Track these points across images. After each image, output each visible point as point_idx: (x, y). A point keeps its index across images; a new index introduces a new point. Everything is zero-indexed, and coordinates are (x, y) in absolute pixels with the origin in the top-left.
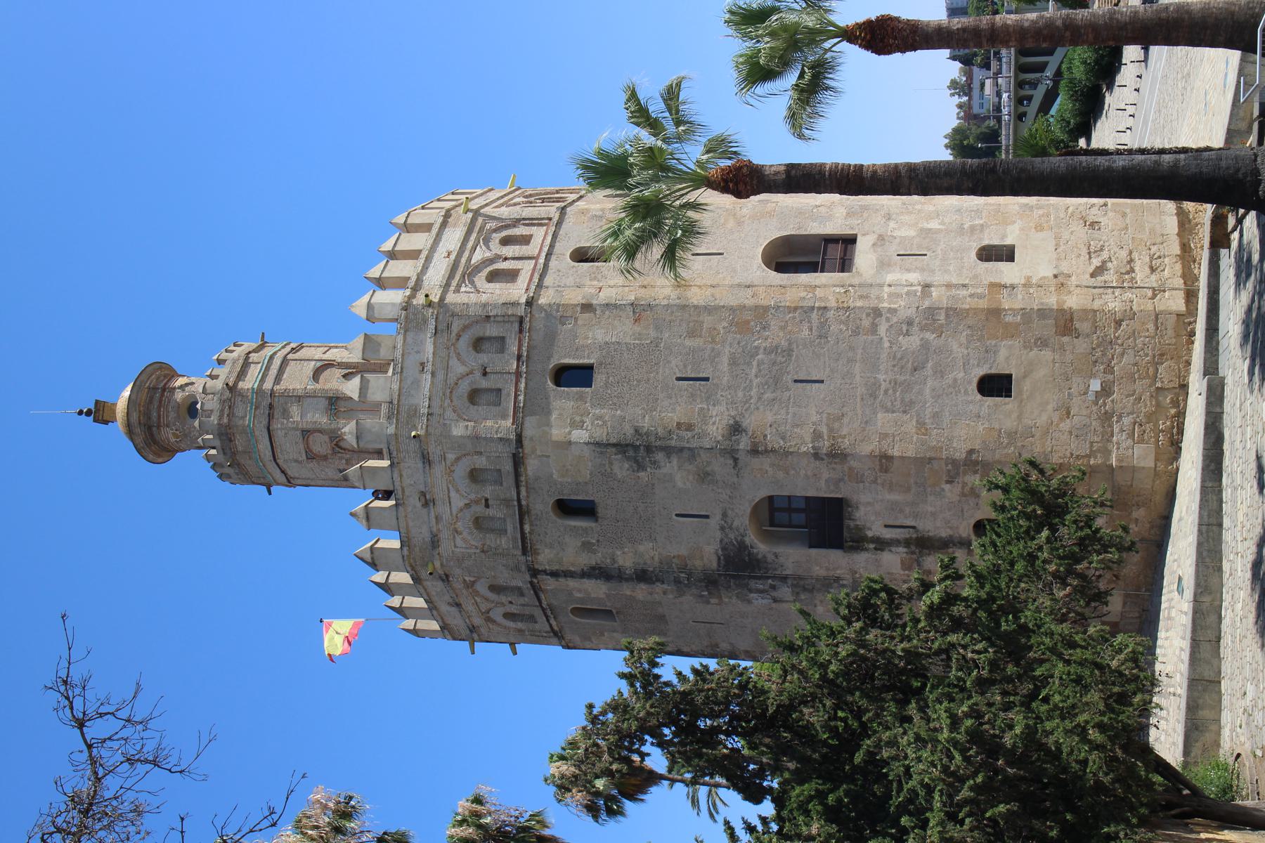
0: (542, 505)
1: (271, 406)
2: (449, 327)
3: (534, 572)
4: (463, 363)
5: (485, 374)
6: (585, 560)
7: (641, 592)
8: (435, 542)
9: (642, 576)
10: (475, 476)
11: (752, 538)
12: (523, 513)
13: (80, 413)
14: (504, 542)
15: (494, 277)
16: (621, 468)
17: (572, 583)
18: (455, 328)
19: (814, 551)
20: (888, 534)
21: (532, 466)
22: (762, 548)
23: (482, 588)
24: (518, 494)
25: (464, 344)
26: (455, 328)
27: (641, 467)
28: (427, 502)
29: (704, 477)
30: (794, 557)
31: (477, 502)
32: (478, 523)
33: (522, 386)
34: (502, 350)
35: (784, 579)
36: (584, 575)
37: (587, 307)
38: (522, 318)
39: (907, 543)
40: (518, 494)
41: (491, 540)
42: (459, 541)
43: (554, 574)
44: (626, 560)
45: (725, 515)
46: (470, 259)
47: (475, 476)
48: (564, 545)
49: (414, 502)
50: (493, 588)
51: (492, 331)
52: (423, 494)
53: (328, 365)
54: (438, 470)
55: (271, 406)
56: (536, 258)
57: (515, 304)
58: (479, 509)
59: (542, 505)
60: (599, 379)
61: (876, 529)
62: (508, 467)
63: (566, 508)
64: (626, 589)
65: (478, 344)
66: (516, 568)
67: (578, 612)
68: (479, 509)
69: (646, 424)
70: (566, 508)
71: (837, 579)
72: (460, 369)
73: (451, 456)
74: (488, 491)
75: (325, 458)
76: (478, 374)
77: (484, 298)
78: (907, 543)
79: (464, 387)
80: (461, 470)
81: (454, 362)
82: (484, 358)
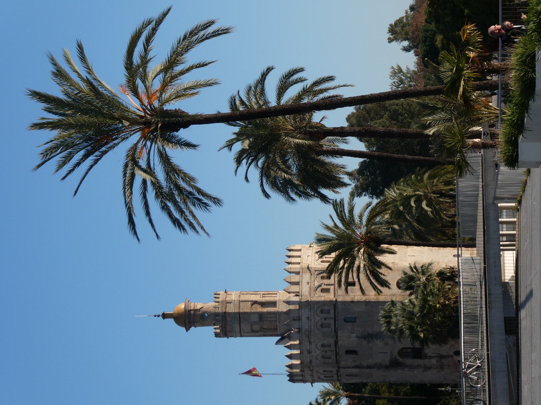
0: (342, 352)
1: (240, 318)
2: (314, 307)
3: (339, 368)
4: (319, 317)
5: (325, 319)
6: (354, 364)
7: (368, 371)
8: (311, 362)
9: (369, 367)
10: (323, 346)
11: (398, 357)
12: (337, 354)
13: (155, 316)
14: (330, 361)
15: (323, 291)
16: (364, 343)
17: (348, 370)
18: (316, 307)
19: (414, 360)
20: (432, 355)
21: (340, 343)
22: (401, 360)
23: (321, 371)
24: (336, 349)
25: (318, 311)
26: (316, 307)
27: (369, 342)
28: (309, 352)
29: (386, 344)
30: (409, 361)
31: (324, 351)
32: (323, 357)
33: (336, 323)
34: (329, 312)
35: (406, 366)
36: (353, 368)
37: (352, 302)
38: (335, 304)
39: (437, 357)
40: (336, 349)
41: (327, 361)
42: (318, 361)
43: (344, 368)
44: (365, 363)
45: (391, 352)
46: (314, 285)
47: (323, 346)
48: (348, 361)
49: (306, 353)
50: (323, 371)
51: (326, 308)
52: (309, 351)
53: (255, 303)
54: (313, 345)
55: (240, 318)
56: (334, 285)
57: (332, 301)
58: (324, 353)
59: (342, 352)
60: (357, 320)
61: (430, 354)
62: (333, 343)
63: (348, 352)
64: (364, 370)
65: (322, 312)
66: (334, 367)
67: (347, 375)
68: (324, 353)
69: (371, 332)
70: (348, 352)
71: (420, 366)
72: (318, 318)
73: (317, 341)
74: (327, 349)
75: (257, 331)
76: (323, 320)
77: (323, 299)
78: (437, 357)
79: (320, 323)
80: (319, 345)
81: (316, 317)
82: (324, 315)
